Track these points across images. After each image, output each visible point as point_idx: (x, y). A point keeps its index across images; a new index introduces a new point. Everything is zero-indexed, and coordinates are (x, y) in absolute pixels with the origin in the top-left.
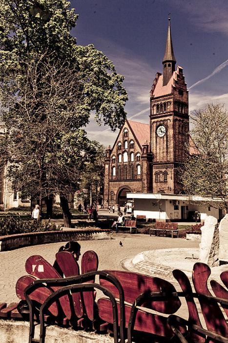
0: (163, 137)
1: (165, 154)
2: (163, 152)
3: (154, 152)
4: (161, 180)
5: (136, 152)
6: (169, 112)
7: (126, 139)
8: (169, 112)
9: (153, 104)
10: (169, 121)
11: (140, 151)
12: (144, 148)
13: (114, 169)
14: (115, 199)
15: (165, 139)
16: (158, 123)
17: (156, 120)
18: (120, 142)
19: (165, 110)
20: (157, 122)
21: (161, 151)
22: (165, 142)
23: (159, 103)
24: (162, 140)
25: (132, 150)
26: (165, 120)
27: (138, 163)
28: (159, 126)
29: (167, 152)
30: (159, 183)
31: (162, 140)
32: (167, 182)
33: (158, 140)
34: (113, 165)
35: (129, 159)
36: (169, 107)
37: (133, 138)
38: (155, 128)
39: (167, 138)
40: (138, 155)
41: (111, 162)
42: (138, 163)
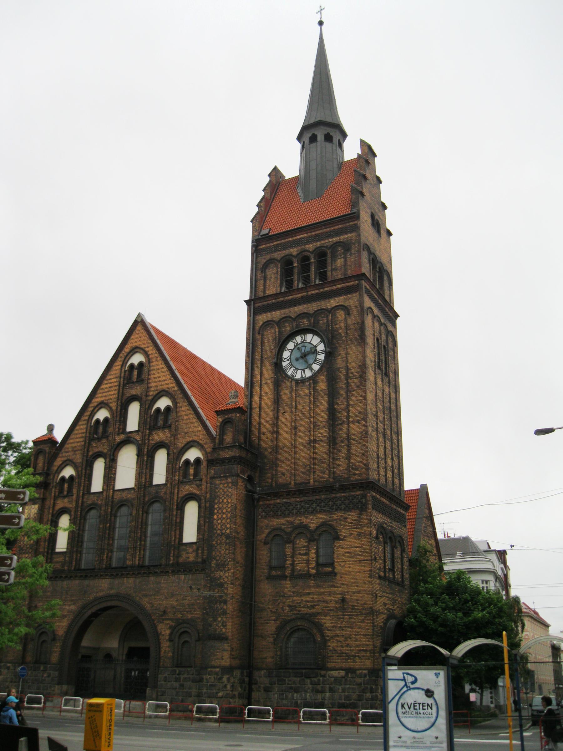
0: (314, 379)
1: (322, 449)
2: (312, 442)
3: (266, 442)
4: (300, 567)
5: (181, 443)
6: (342, 280)
7: (136, 390)
8: (342, 280)
9: (263, 260)
10: (341, 315)
11: (200, 435)
12: (225, 423)
13: (65, 521)
14: (55, 658)
15: (322, 385)
16: (288, 328)
17: (277, 315)
18: (102, 405)
19: (323, 276)
20: (280, 323)
21: (302, 439)
22: (324, 403)
23: (294, 251)
24: (304, 391)
25: (160, 436)
26: (321, 311)
27: (187, 489)
28: (291, 337)
29: (333, 441)
30: (288, 584)
31: (304, 391)
32: (333, 574)
33: (285, 393)
34: (61, 503)
35: (139, 475)
36: (340, 262)
37: (171, 385)
38: (270, 346)
39: (332, 380)
40: (193, 454)
41: (54, 491)
42: (187, 489)
